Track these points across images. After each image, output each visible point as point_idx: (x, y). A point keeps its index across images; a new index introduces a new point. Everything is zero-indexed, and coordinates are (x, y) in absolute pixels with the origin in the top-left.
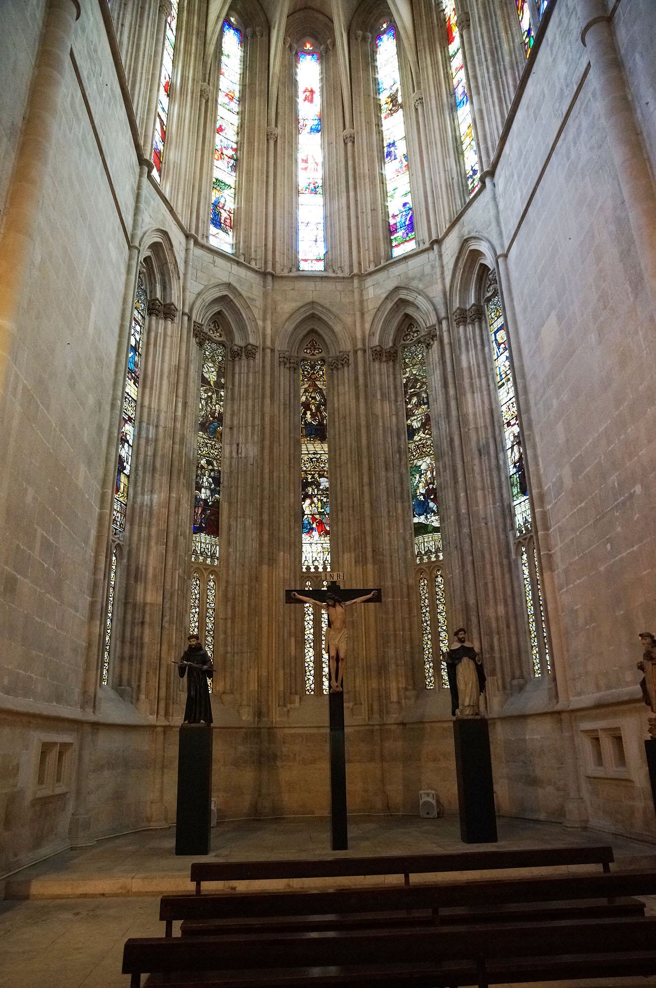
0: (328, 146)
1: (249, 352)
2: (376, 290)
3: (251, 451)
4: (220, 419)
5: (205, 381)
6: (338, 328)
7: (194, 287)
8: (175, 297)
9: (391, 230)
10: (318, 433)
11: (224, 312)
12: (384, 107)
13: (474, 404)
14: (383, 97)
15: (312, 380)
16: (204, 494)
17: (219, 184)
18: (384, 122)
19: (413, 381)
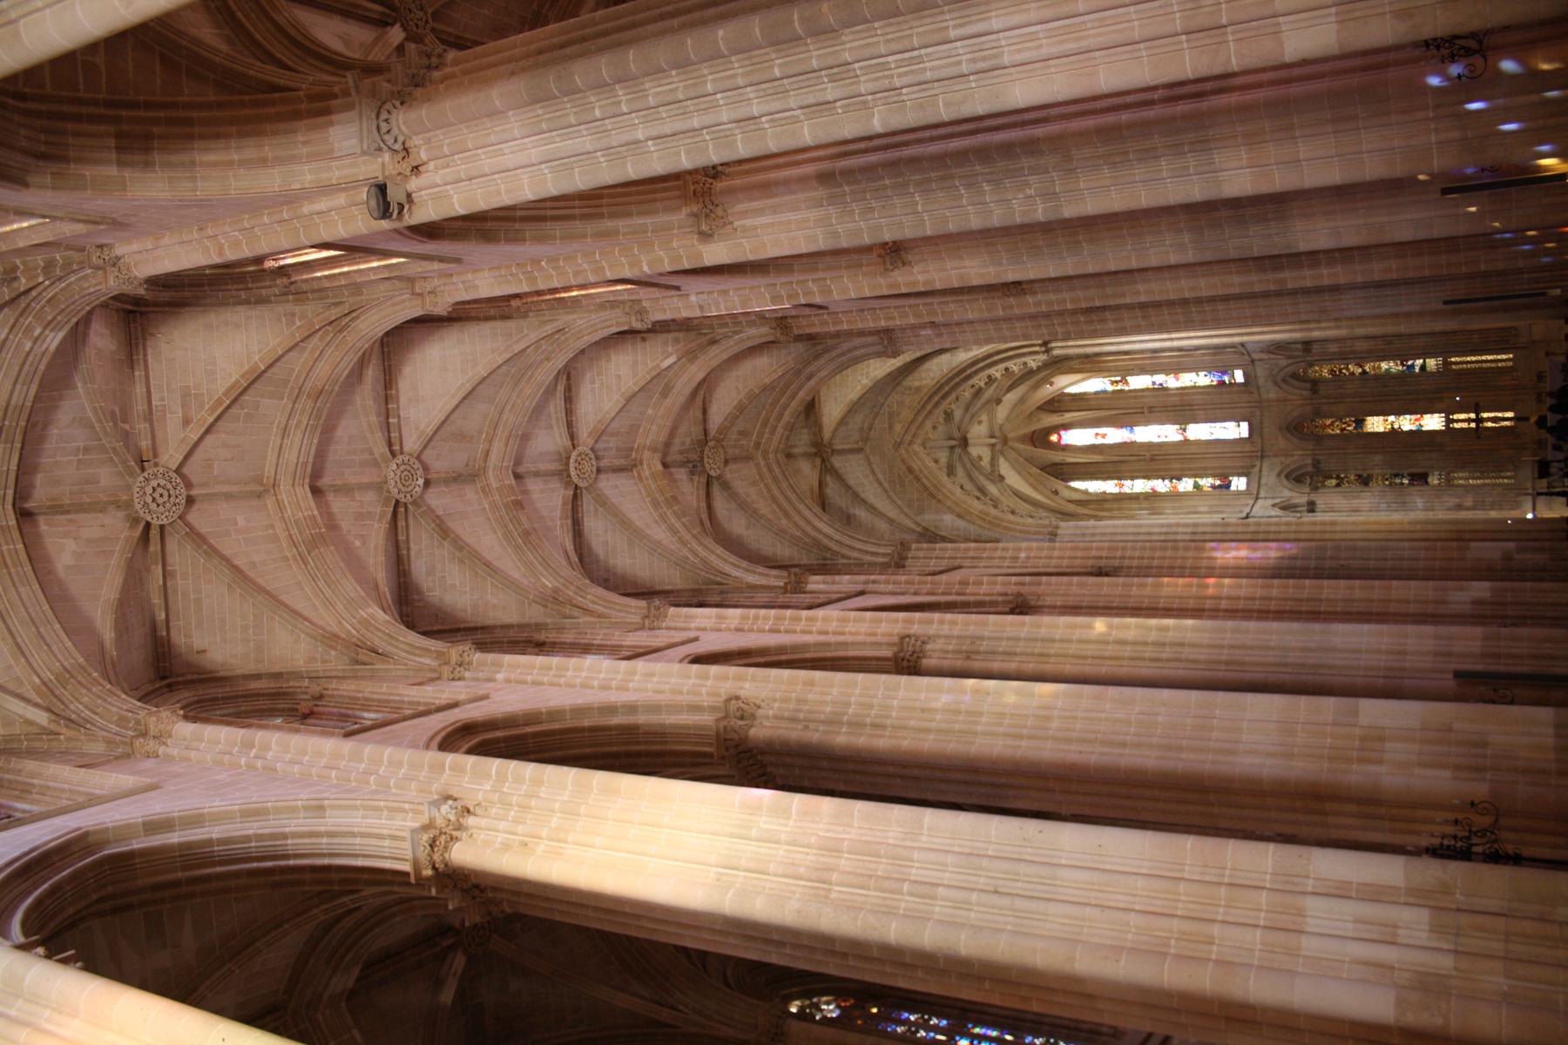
0: (1147, 423)
1: (1316, 463)
2: (1272, 394)
3: (1378, 458)
4: (1360, 476)
5: (1338, 485)
6: (1295, 414)
7: (1287, 493)
8: (1303, 500)
9: (1222, 383)
10: (1360, 423)
11: (1295, 478)
12: (1119, 387)
13: (1361, 346)
14: (1110, 388)
15: (1326, 426)
16: (1406, 481)
17: (1196, 486)
18: (1132, 387)
19: (1332, 372)
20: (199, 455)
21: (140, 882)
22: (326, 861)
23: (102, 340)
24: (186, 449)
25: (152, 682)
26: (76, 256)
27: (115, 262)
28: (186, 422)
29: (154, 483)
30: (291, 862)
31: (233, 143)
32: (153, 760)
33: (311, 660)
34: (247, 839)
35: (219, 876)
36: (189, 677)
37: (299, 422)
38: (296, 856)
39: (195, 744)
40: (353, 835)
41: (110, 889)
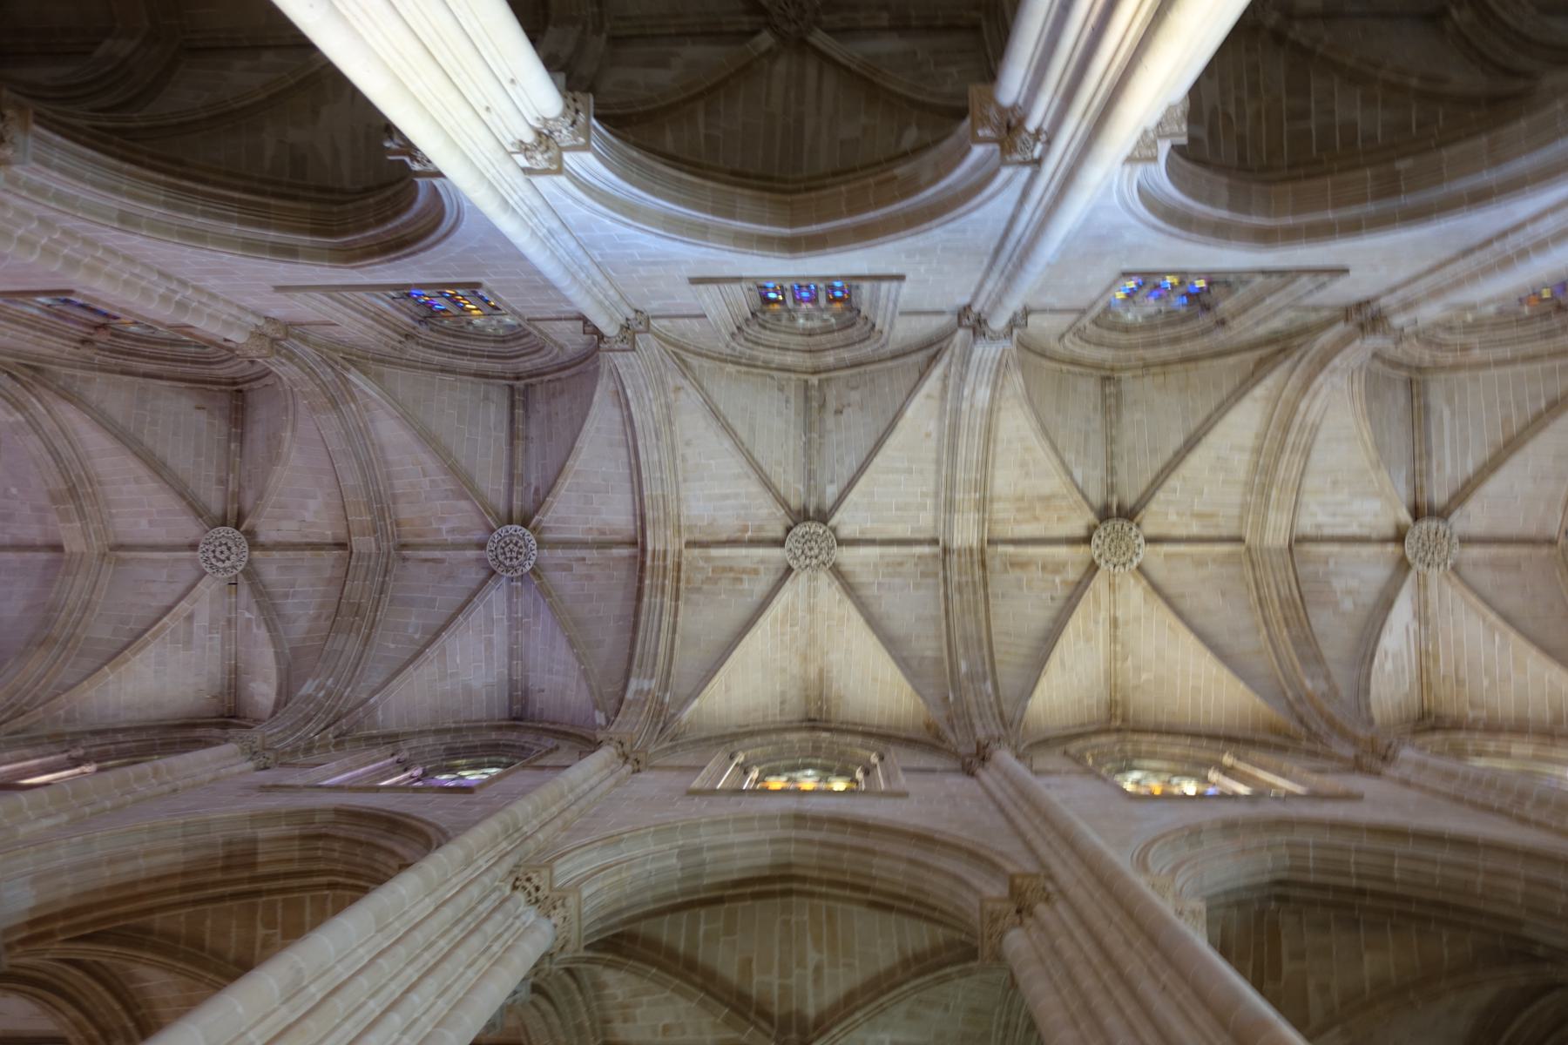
20: (180, 588)
21: (308, 207)
22: (126, 166)
23: (263, 690)
24: (194, 593)
25: (251, 390)
26: (287, 759)
27: (254, 754)
28: (190, 618)
29: (228, 564)
30: (162, 177)
31: (143, 875)
32: (271, 315)
33: (87, 381)
34: (204, 214)
35: (234, 188)
36: (215, 388)
37: (70, 614)
38: (157, 182)
39: (231, 319)
40: (93, 183)
41: (335, 209)
